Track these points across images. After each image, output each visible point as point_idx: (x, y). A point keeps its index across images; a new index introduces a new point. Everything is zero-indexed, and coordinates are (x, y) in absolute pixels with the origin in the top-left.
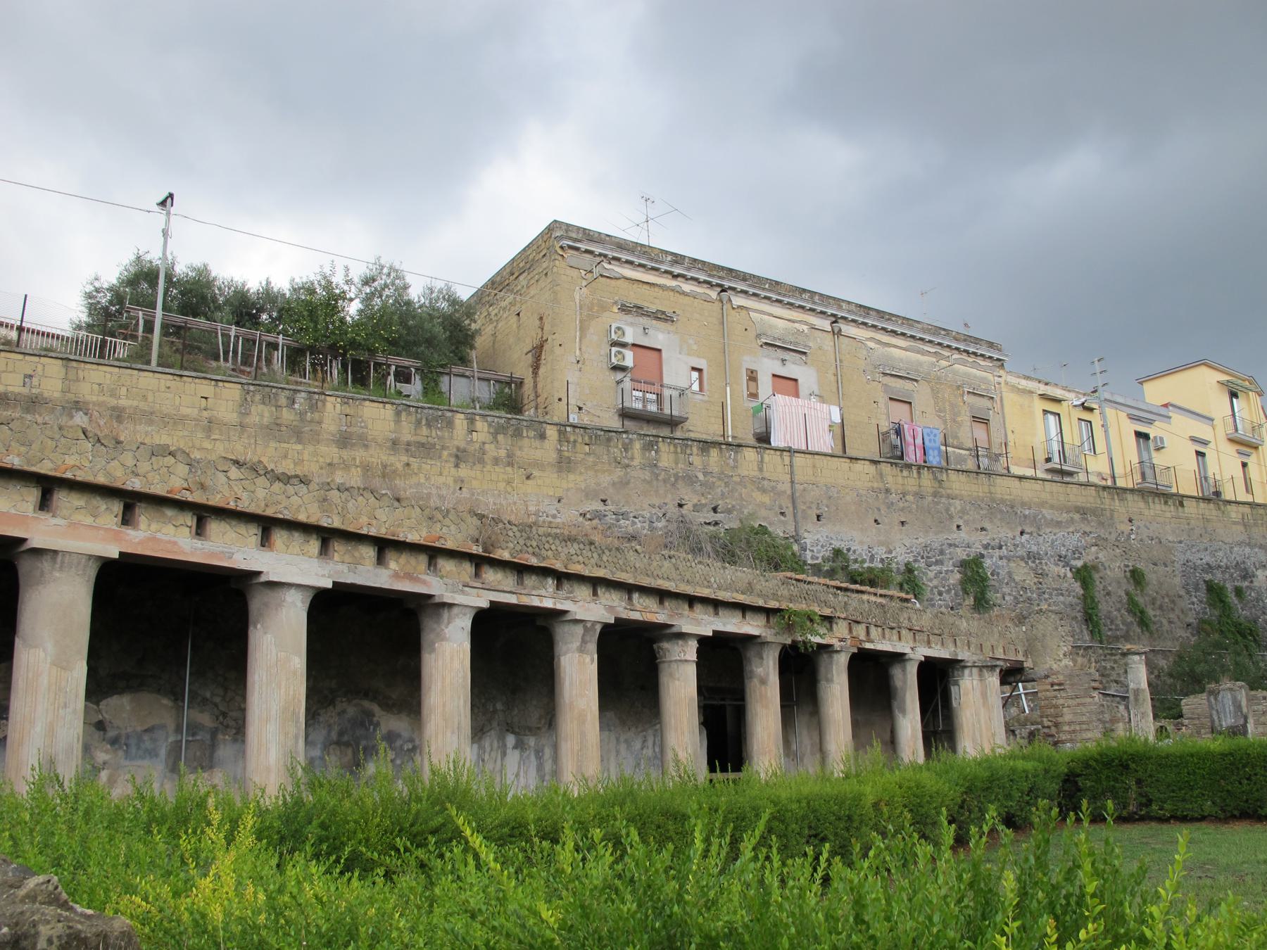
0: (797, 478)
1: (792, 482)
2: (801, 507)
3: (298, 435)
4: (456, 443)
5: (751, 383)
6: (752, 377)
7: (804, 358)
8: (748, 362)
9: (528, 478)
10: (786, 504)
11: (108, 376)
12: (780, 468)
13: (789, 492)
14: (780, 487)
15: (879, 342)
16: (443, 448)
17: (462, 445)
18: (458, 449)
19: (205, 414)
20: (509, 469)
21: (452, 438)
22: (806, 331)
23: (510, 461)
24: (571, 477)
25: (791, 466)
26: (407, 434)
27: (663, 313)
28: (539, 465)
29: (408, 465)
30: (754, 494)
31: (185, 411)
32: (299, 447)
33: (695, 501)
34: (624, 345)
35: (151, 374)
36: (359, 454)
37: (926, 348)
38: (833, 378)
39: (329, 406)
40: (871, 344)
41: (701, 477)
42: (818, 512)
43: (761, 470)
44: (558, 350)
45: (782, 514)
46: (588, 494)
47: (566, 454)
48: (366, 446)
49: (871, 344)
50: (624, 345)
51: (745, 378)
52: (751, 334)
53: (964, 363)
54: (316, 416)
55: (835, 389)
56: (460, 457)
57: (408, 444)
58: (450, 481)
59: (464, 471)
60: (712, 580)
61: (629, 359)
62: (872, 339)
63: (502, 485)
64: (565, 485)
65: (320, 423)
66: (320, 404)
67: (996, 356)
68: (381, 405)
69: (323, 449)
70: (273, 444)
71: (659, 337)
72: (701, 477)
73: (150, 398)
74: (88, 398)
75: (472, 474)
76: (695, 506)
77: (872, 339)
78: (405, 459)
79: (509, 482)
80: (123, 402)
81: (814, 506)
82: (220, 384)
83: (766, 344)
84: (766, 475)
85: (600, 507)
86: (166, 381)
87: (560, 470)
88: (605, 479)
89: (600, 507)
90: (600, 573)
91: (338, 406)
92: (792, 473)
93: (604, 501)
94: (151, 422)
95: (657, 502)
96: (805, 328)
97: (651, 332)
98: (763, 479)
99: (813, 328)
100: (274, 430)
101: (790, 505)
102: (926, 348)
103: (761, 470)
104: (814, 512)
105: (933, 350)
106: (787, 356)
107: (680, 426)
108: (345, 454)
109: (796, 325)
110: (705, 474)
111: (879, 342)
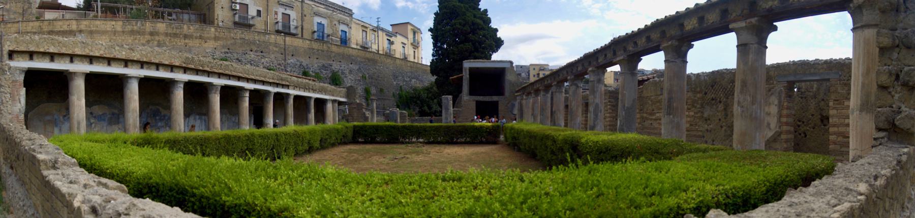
0: (286, 44)
1: (285, 44)
3: (138, 33)
4: (184, 33)
6: (276, 13)
8: (275, 9)
9: (206, 42)
10: (283, 51)
12: (281, 41)
15: (316, 6)
16: (181, 34)
17: (187, 33)
18: (185, 35)
19: (113, 30)
20: (200, 40)
21: (183, 31)
23: (201, 37)
24: (219, 42)
26: (170, 31)
28: (209, 38)
29: (170, 39)
31: (108, 29)
34: (236, 3)
36: (157, 38)
39: (147, 24)
40: (313, 6)
41: (258, 42)
43: (276, 41)
44: (216, 5)
46: (223, 47)
47: (217, 35)
48: (158, 35)
49: (313, 6)
50: (236, 3)
54: (144, 27)
56: (186, 37)
57: (170, 33)
58: (183, 44)
59: (186, 41)
61: (238, 7)
62: (314, 5)
63: (198, 45)
64: (217, 44)
65: (145, 29)
69: (146, 36)
70: (132, 36)
77: (314, 5)
78: (169, 38)
79: (200, 44)
80: (92, 29)
84: (277, 42)
85: (228, 51)
86: (103, 22)
87: (215, 40)
88: (229, 43)
89: (228, 51)
94: (100, 33)
95: (244, 49)
100: (132, 32)
102: (330, 9)
103: (276, 41)
106: (287, 8)
108: (152, 37)
110: (259, 41)
111: (316, 6)
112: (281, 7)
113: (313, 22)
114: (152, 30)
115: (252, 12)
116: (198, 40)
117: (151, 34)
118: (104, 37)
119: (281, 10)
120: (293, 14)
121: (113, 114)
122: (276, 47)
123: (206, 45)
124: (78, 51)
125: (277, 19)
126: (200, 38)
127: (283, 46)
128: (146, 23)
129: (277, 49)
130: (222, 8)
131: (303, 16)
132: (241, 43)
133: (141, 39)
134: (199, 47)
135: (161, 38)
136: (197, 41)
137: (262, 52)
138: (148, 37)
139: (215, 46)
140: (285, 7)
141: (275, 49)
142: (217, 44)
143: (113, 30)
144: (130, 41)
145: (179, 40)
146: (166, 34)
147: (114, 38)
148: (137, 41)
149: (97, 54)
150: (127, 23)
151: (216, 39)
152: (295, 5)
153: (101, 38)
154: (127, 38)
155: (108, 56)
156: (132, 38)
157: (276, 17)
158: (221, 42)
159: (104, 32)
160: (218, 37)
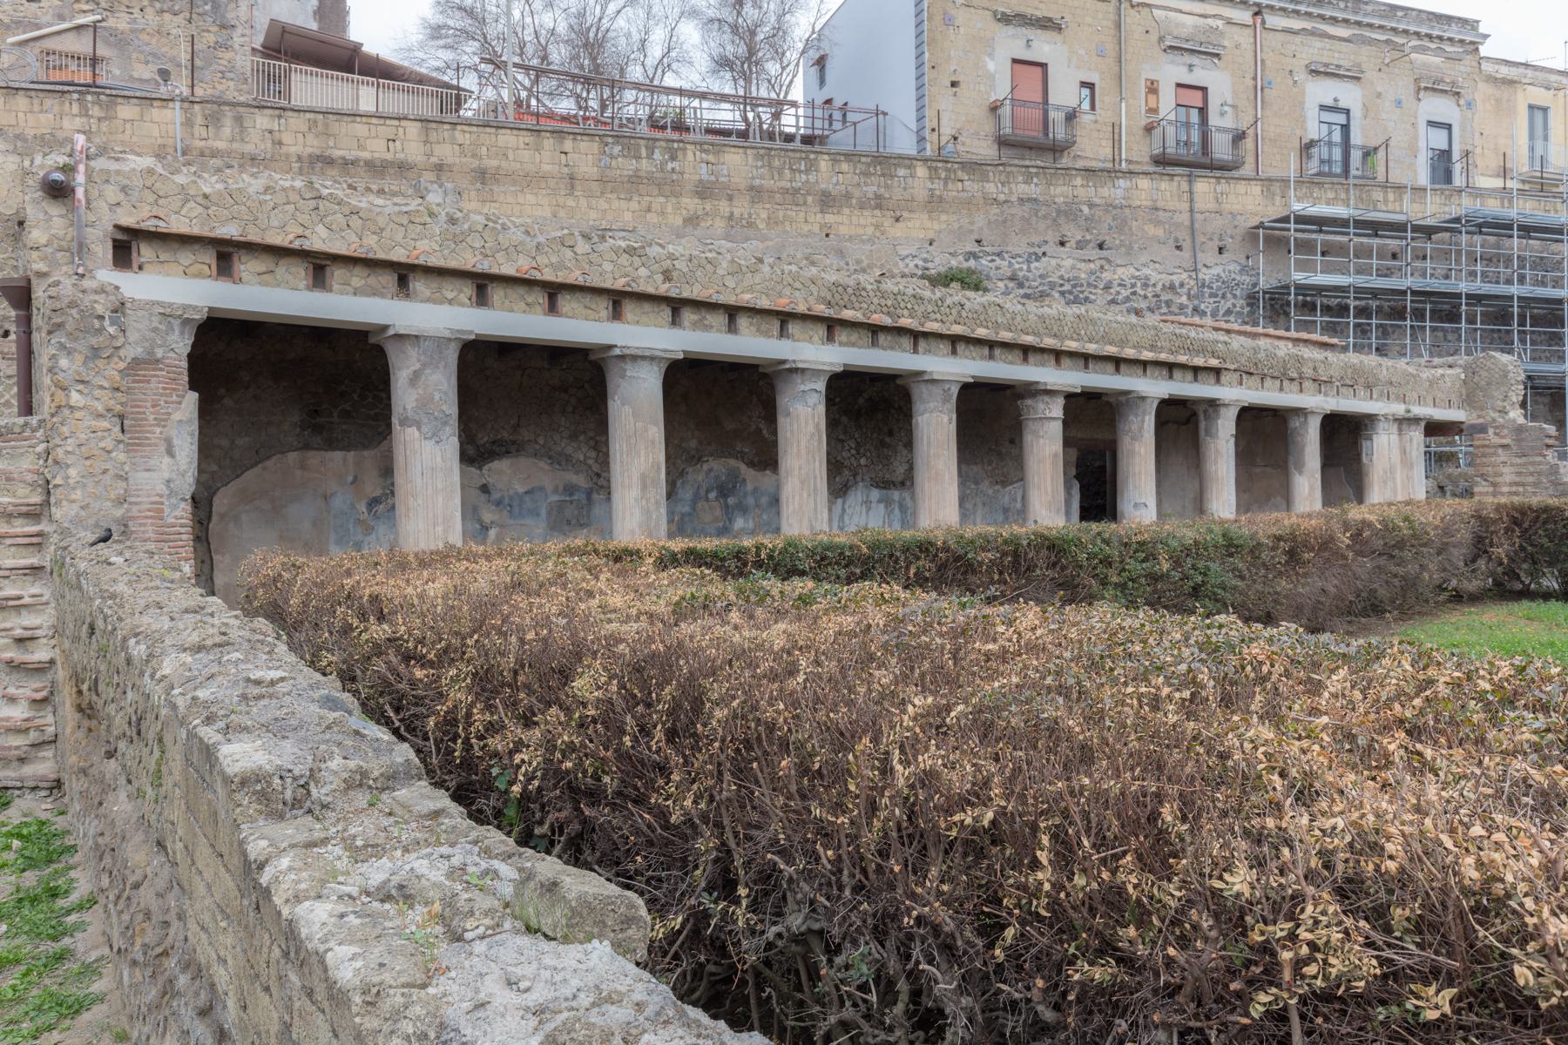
0: (1198, 206)
1: (1191, 211)
2: (1200, 238)
5: (1150, 96)
6: (1153, 89)
7: (1216, 61)
9: (897, 220)
10: (1183, 235)
11: (467, 135)
13: (1187, 223)
14: (1178, 218)
20: (877, 212)
22: (1221, 27)
23: (879, 203)
24: (944, 217)
25: (1191, 192)
27: (1050, 20)
30: (1146, 227)
31: (546, 168)
32: (662, 199)
33: (1079, 238)
35: (509, 131)
37: (1374, 36)
38: (1250, 83)
41: (1086, 210)
42: (1221, 244)
45: (1178, 248)
51: (1143, 90)
52: (1154, 37)
53: (1424, 50)
55: (1252, 97)
58: (816, 229)
60: (1083, 332)
63: (870, 230)
64: (936, 226)
66: (680, 154)
67: (1468, 39)
68: (741, 150)
70: (636, 198)
71: (1044, 47)
72: (1086, 210)
73: (511, 157)
74: (450, 160)
75: (838, 218)
76: (1078, 242)
79: (877, 226)
81: (1216, 238)
82: (579, 137)
83: (1171, 47)
85: (976, 249)
89: (976, 249)
90: (957, 329)
91: (698, 153)
92: (1192, 200)
93: (978, 242)
94: (514, 183)
95: (1036, 239)
96: (1220, 23)
97: (1034, 44)
98: (1157, 209)
99: (1229, 22)
101: (1189, 241)
104: (1216, 243)
105: (1384, 38)
106: (1195, 60)
107: (1066, 153)
109: (1210, 21)
112: (1172, 62)
113: (1302, 103)
114: (705, 177)
115: (1065, 93)
116: (866, 213)
117: (704, 191)
118: (531, 198)
119: (1172, 72)
120: (1219, 82)
121: (570, 489)
122: (1158, 223)
123: (898, 231)
124: (427, 250)
125: (1155, 111)
126: (879, 207)
127: (1185, 218)
128: (684, 150)
129: (1160, 232)
130: (954, 84)
131: (1259, 90)
132: (1023, 218)
133: (669, 210)
134: (871, 240)
135: (741, 208)
136: (867, 218)
137: (1101, 246)
138: (691, 203)
139: (931, 235)
140: (1188, 59)
141: (1151, 230)
142: (936, 226)
143: (566, 170)
144: (628, 216)
145: (802, 215)
146: (756, 193)
147: (570, 202)
148: (653, 218)
149: (508, 270)
150: (617, 149)
151: (934, 203)
152: (1226, 43)
153: (521, 200)
154: (616, 204)
155: (548, 275)
156: (634, 205)
157: (1152, 104)
158: (953, 218)
159: (531, 180)
160: (941, 199)
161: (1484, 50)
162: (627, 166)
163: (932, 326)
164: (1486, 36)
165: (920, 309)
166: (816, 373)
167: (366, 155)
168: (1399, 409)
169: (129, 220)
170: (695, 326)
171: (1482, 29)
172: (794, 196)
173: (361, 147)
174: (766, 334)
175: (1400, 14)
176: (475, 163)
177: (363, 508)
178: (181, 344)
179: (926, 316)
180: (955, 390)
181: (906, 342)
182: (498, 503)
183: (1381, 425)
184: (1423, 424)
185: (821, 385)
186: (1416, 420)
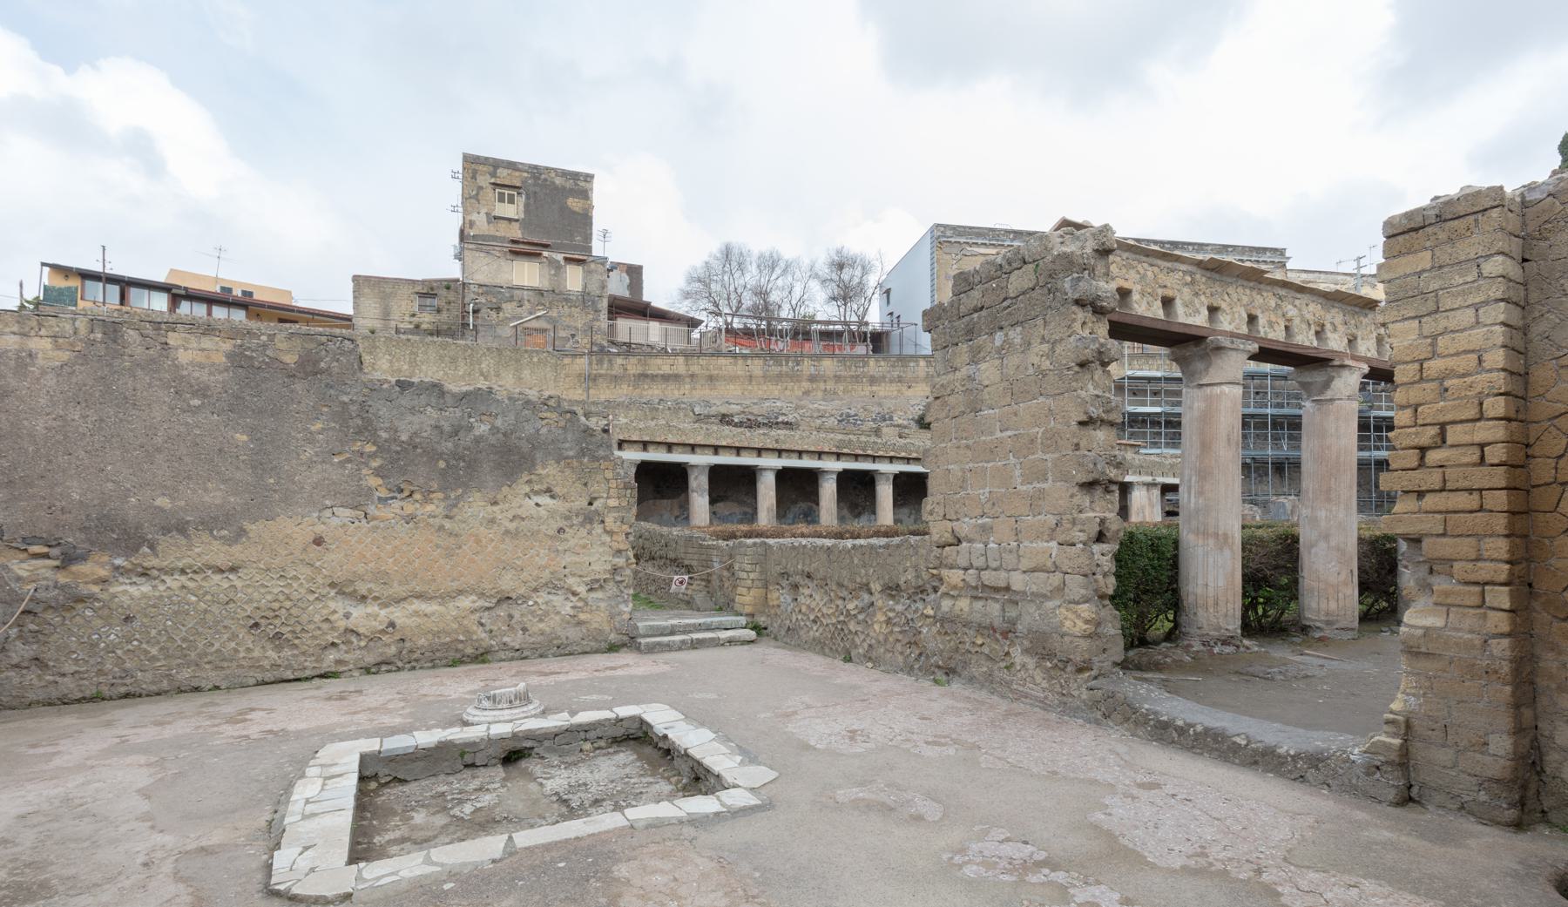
9: (909, 387)
23: (900, 380)
58: (868, 393)
79: (899, 391)
90: (892, 454)
116: (894, 385)
118: (732, 387)
123: (910, 393)
126: (900, 381)
134: (896, 398)
135: (830, 386)
136: (894, 387)
138: (806, 385)
144: (776, 392)
146: (838, 378)
148: (788, 393)
154: (771, 387)
159: (733, 379)
161: (1289, 266)
162: (775, 370)
163: (881, 453)
164: (1289, 258)
165: (876, 447)
166: (832, 472)
167: (662, 372)
168: (1149, 479)
169: (621, 438)
170: (787, 457)
171: (1287, 255)
172: (856, 379)
173: (660, 369)
174: (813, 459)
175: (1230, 249)
176: (708, 373)
177: (673, 519)
178: (634, 470)
179: (879, 449)
180: (891, 477)
181: (870, 459)
182: (719, 518)
183: (1136, 488)
184: (1159, 487)
185: (835, 477)
186: (1154, 485)
